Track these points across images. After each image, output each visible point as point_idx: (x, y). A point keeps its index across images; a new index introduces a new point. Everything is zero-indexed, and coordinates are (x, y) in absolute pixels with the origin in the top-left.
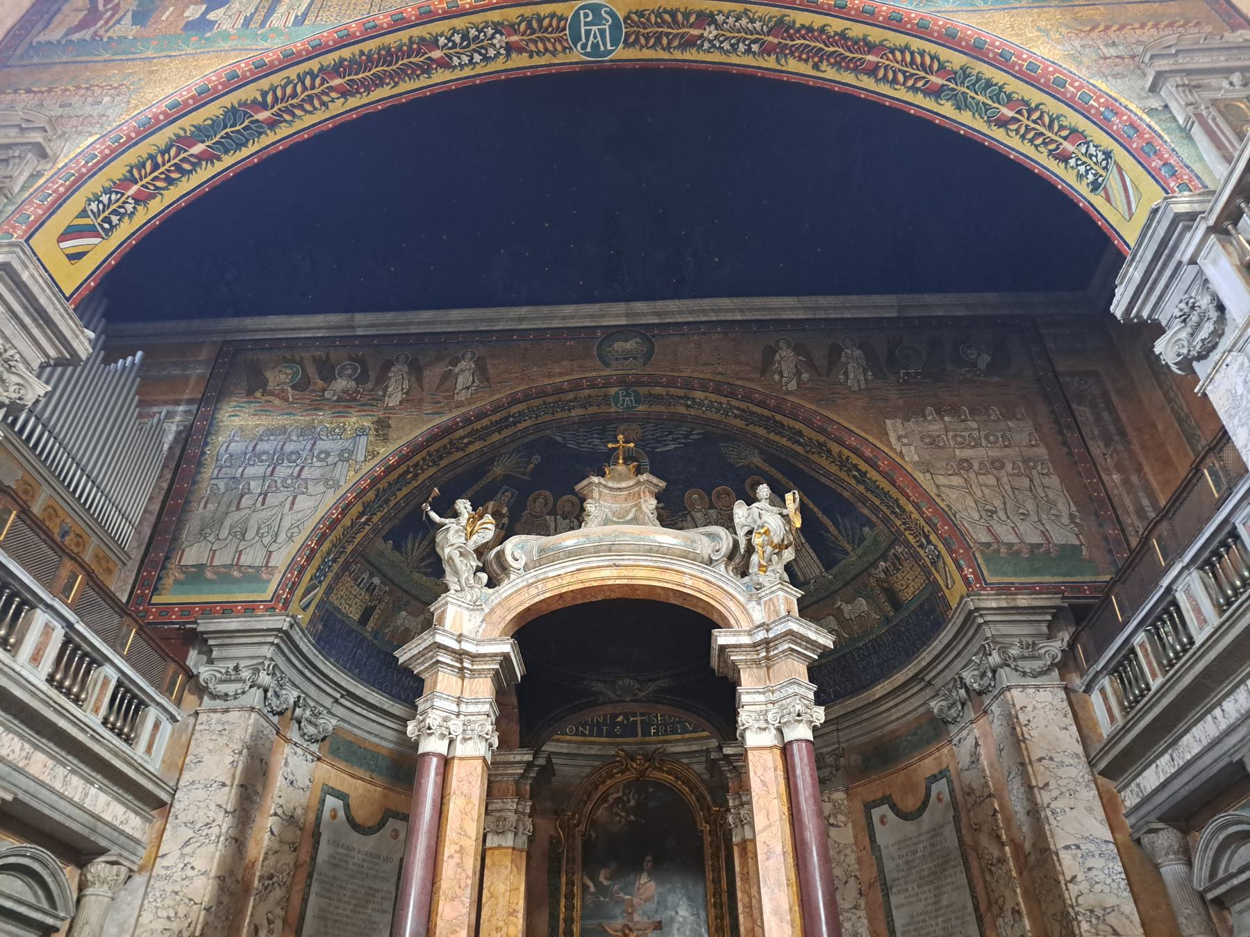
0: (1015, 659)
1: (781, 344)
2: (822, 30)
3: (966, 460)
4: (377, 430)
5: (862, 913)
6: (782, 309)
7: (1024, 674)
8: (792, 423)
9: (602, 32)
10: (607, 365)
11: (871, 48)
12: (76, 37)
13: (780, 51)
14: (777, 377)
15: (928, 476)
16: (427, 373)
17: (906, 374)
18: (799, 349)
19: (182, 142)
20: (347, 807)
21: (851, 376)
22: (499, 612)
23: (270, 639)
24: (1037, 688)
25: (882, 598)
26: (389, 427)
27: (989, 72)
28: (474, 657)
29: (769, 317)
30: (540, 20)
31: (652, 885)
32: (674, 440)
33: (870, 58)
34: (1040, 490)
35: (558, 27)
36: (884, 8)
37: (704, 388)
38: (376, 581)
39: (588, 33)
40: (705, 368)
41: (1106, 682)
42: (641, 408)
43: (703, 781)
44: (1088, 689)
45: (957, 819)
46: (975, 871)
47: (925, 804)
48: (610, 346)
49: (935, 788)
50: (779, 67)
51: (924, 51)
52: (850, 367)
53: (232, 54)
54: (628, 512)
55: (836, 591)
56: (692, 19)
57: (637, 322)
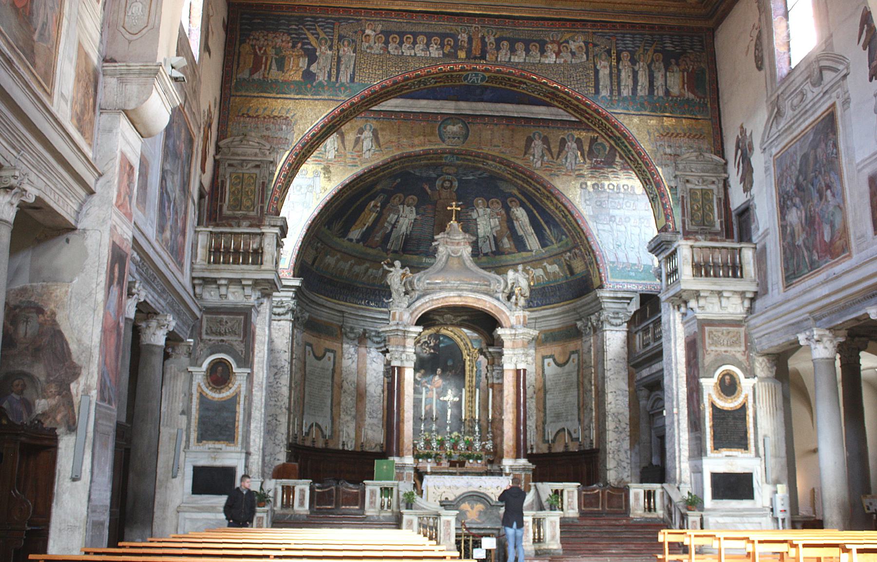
0: (611, 318)
1: (536, 136)
2: (569, 101)
3: (614, 216)
4: (324, 174)
5: (534, 400)
6: (540, 114)
7: (613, 325)
8: (536, 184)
9: (477, 80)
10: (444, 141)
11: (588, 113)
12: (256, 76)
13: (552, 99)
14: (531, 158)
15: (595, 224)
16: (347, 137)
17: (596, 161)
18: (545, 140)
19: (312, 143)
20: (312, 349)
21: (569, 160)
22: (416, 313)
23: (293, 290)
24: (617, 331)
25: (566, 268)
26: (330, 172)
27: (626, 144)
28: (409, 332)
29: (532, 116)
30: (452, 76)
31: (441, 381)
34: (643, 235)
37: (492, 160)
38: (319, 245)
41: (641, 333)
42: (459, 162)
43: (468, 336)
44: (636, 333)
45: (578, 371)
46: (581, 392)
47: (567, 362)
48: (445, 128)
49: (573, 356)
52: (569, 155)
53: (331, 103)
54: (458, 251)
55: (545, 258)
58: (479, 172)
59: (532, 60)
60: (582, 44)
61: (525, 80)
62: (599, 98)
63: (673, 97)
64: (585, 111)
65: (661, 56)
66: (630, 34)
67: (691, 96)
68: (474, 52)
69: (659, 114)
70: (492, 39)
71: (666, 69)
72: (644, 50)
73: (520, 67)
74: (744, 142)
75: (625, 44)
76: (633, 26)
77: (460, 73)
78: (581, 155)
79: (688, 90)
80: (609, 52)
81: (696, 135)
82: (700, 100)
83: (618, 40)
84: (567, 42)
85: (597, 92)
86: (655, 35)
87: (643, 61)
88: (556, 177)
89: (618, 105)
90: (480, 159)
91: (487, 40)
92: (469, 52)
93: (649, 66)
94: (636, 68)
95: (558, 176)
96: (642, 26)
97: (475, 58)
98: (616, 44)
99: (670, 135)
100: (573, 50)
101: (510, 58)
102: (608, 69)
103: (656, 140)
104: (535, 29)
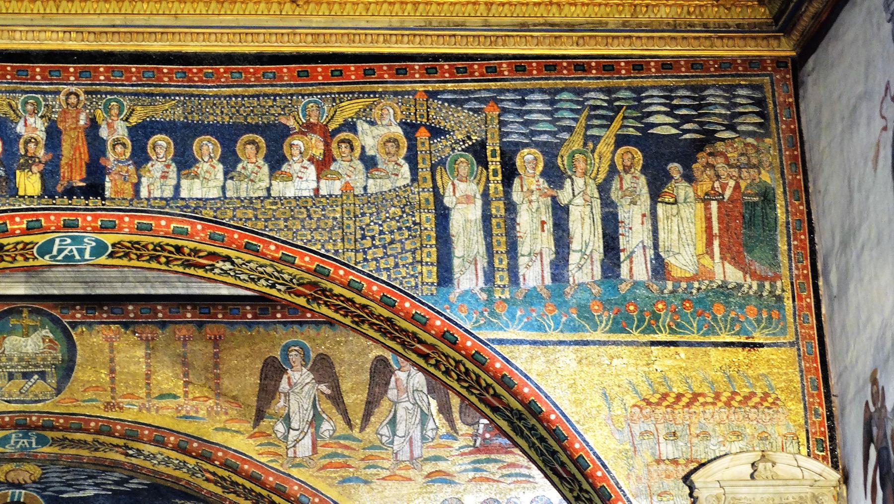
1: (294, 356)
2: (364, 307)
9: (81, 252)
11: (421, 342)
14: (280, 428)
21: (401, 430)
32: (97, 485)
33: (419, 346)
35: (22, 249)
36: (438, 323)
39: (60, 251)
40: (162, 403)
42: (46, 449)
50: (309, 307)
51: (480, 376)
52: (401, 413)
56: (201, 254)
57: (45, 292)
58: (116, 476)
59: (245, 190)
60: (398, 131)
61: (224, 252)
62: (454, 295)
63: (677, 281)
64: (415, 335)
65: (639, 156)
66: (542, 91)
67: (734, 275)
68: (64, 171)
69: (636, 336)
70: (121, 130)
71: (656, 195)
72: (587, 138)
73: (208, 214)
74: (882, 427)
75: (526, 123)
76: (550, 64)
77: (27, 239)
78: (440, 411)
79: (723, 258)
80: (479, 152)
81: (753, 394)
82: (761, 287)
83: (504, 111)
84: (351, 126)
85: (445, 277)
86: (618, 89)
87: (585, 174)
88: (363, 488)
89: (513, 317)
90: (116, 441)
91: (104, 133)
92: (49, 175)
93: (604, 189)
94: (564, 196)
95: (366, 482)
96: (580, 65)
97: (70, 192)
98: (502, 124)
99: (671, 399)
100: (370, 152)
101: (177, 188)
102: (479, 203)
103: (631, 420)
104: (252, 91)
